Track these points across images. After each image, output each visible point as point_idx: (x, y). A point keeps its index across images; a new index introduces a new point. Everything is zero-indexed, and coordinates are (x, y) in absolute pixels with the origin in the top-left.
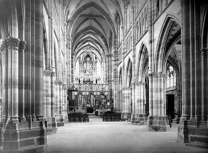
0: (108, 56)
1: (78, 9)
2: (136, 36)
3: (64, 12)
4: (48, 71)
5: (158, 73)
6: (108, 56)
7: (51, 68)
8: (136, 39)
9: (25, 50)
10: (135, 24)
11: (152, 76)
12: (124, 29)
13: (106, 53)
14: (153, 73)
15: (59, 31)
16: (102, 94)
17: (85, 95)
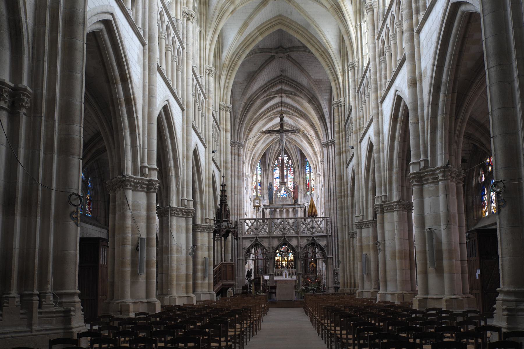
0: (327, 145)
1: (242, 38)
2: (381, 80)
3: (208, 43)
4: (139, 177)
5: (438, 169)
6: (327, 145)
7: (147, 169)
8: (381, 86)
9: (29, 109)
10: (377, 50)
11: (422, 177)
12: (356, 68)
13: (324, 140)
14: (424, 168)
15: (185, 84)
16: (314, 244)
17: (269, 248)
